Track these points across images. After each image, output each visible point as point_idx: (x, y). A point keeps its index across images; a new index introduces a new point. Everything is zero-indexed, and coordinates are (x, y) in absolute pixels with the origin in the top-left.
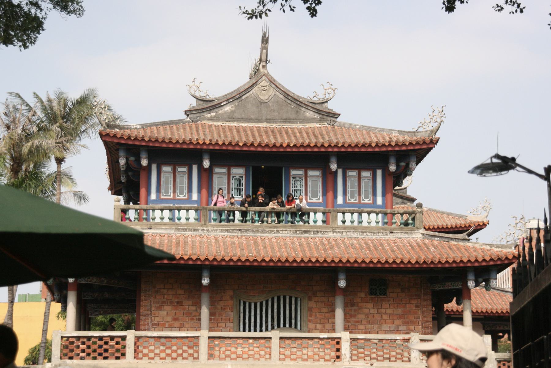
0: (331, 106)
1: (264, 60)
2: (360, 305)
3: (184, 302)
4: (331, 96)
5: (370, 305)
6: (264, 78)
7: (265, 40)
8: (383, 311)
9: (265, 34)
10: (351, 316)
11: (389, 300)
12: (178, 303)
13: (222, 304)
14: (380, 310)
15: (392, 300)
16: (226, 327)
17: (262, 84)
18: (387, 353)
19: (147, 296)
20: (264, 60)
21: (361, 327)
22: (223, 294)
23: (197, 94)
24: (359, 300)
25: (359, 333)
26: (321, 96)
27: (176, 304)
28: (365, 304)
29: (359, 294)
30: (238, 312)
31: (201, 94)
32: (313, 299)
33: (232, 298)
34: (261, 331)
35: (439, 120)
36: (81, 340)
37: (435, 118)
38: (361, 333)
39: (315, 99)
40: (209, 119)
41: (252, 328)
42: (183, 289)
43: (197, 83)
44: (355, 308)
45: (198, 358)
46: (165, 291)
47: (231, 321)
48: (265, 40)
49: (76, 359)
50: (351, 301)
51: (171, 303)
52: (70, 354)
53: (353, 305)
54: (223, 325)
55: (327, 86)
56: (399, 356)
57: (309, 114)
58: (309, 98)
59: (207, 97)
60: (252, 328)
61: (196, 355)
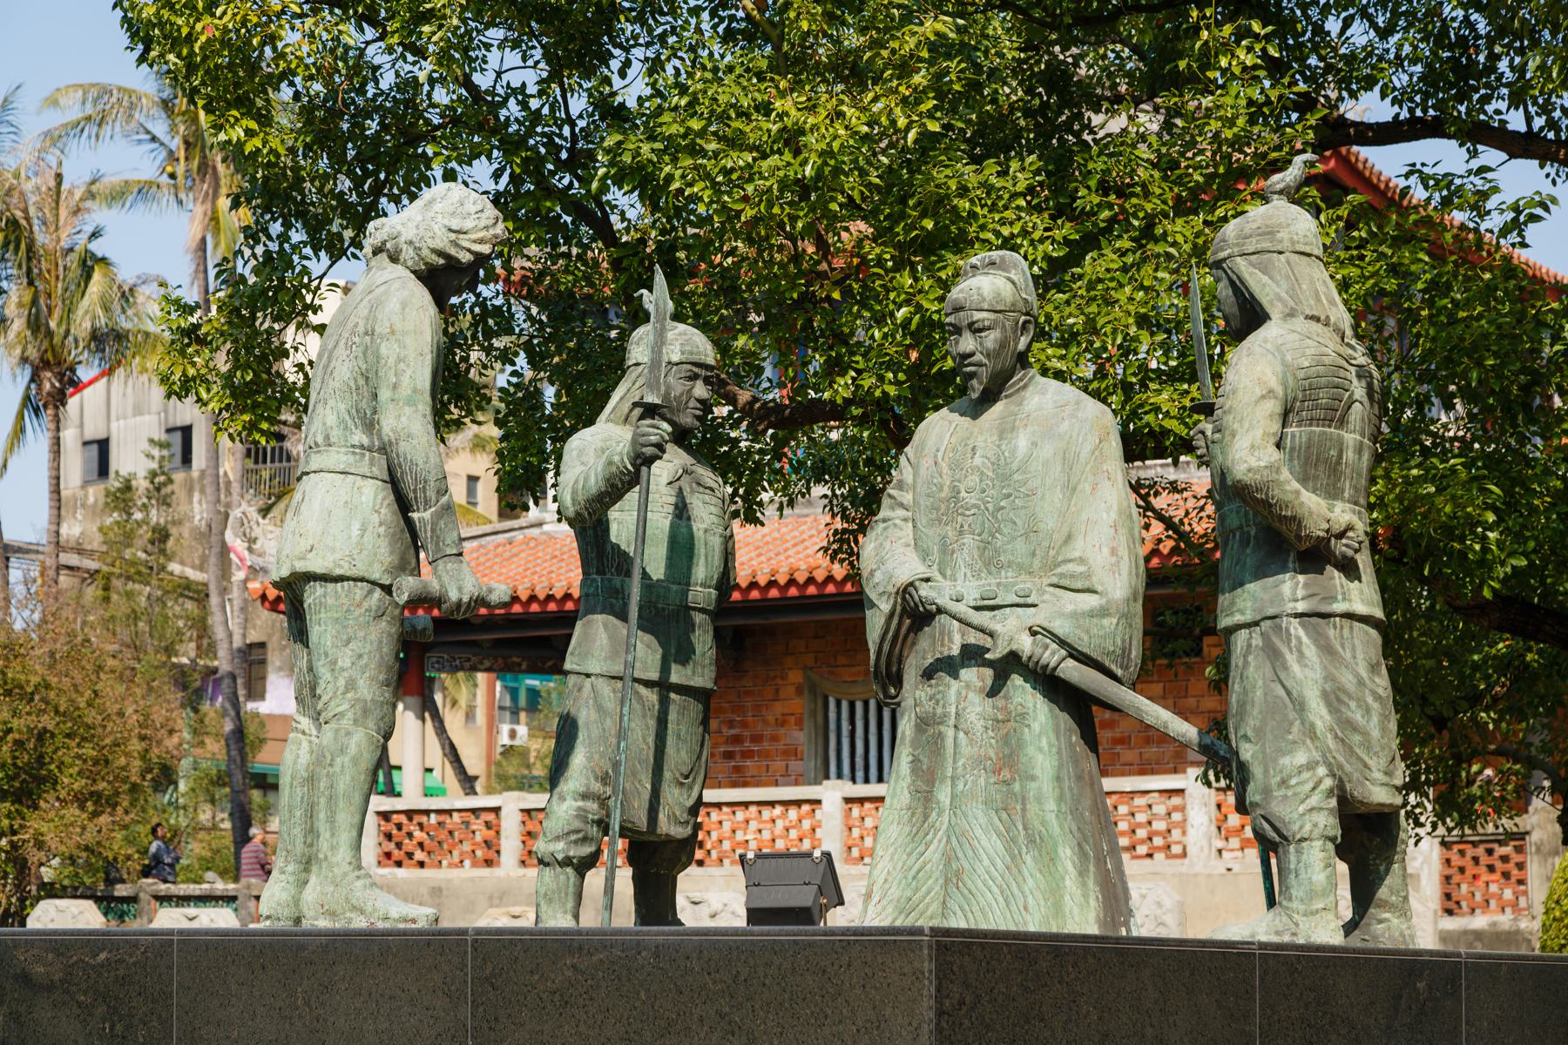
13: (779, 708)
16: (786, 775)
18: (1157, 833)
21: (1129, 755)
22: (780, 682)
25: (1123, 774)
30: (821, 732)
33: (799, 691)
34: (867, 781)
36: (417, 819)
38: (1130, 774)
41: (860, 774)
49: (409, 866)
52: (396, 854)
54: (778, 765)
56: (1158, 841)
60: (860, 774)
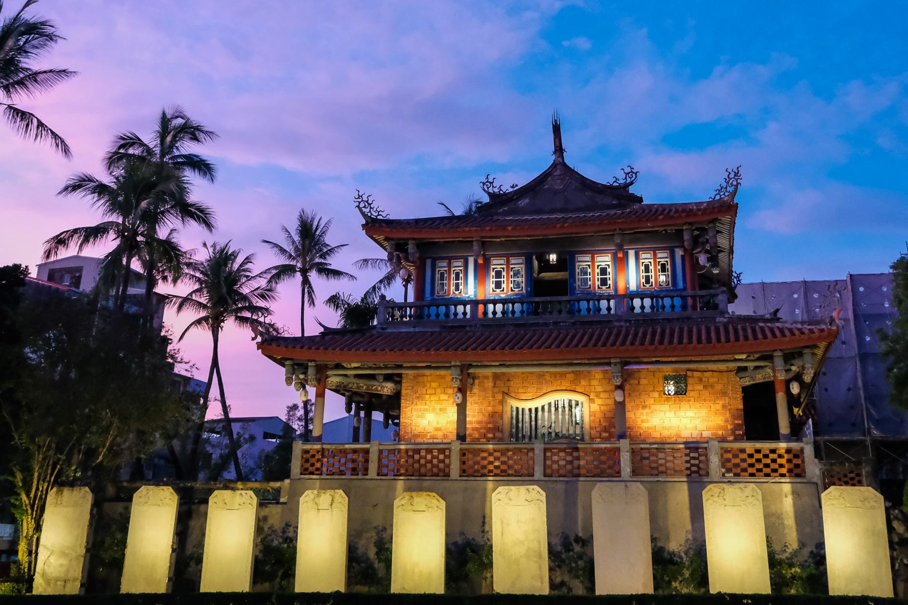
0: (632, 190)
1: (559, 150)
2: (653, 407)
3: (448, 408)
4: (632, 179)
5: (666, 407)
6: (559, 167)
7: (557, 129)
8: (682, 413)
9: (556, 123)
10: (643, 421)
11: (689, 401)
12: (441, 410)
14: (678, 413)
15: (692, 399)
17: (555, 174)
19: (408, 402)
20: (559, 150)
23: (491, 190)
24: (651, 401)
26: (622, 182)
27: (438, 411)
28: (659, 406)
29: (651, 394)
31: (496, 190)
32: (596, 402)
35: (735, 183)
37: (730, 182)
39: (615, 184)
40: (499, 214)
42: (447, 394)
43: (491, 180)
44: (647, 410)
45: (448, 475)
46: (427, 396)
47: (500, 430)
48: (557, 129)
50: (641, 402)
51: (434, 410)
53: (644, 407)
55: (628, 170)
57: (609, 200)
58: (608, 184)
59: (501, 192)
61: (447, 470)
